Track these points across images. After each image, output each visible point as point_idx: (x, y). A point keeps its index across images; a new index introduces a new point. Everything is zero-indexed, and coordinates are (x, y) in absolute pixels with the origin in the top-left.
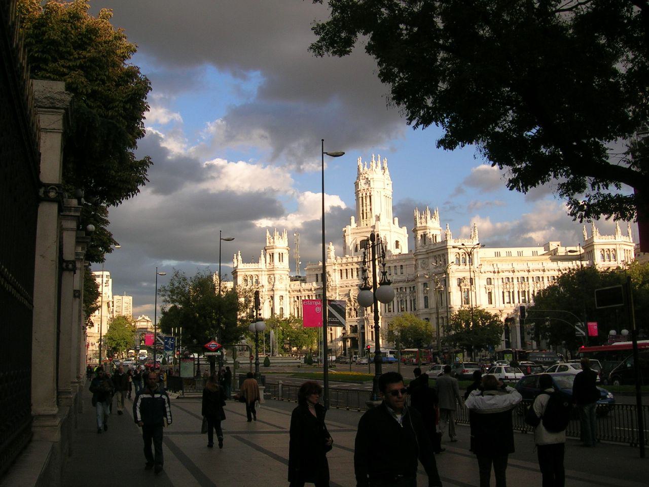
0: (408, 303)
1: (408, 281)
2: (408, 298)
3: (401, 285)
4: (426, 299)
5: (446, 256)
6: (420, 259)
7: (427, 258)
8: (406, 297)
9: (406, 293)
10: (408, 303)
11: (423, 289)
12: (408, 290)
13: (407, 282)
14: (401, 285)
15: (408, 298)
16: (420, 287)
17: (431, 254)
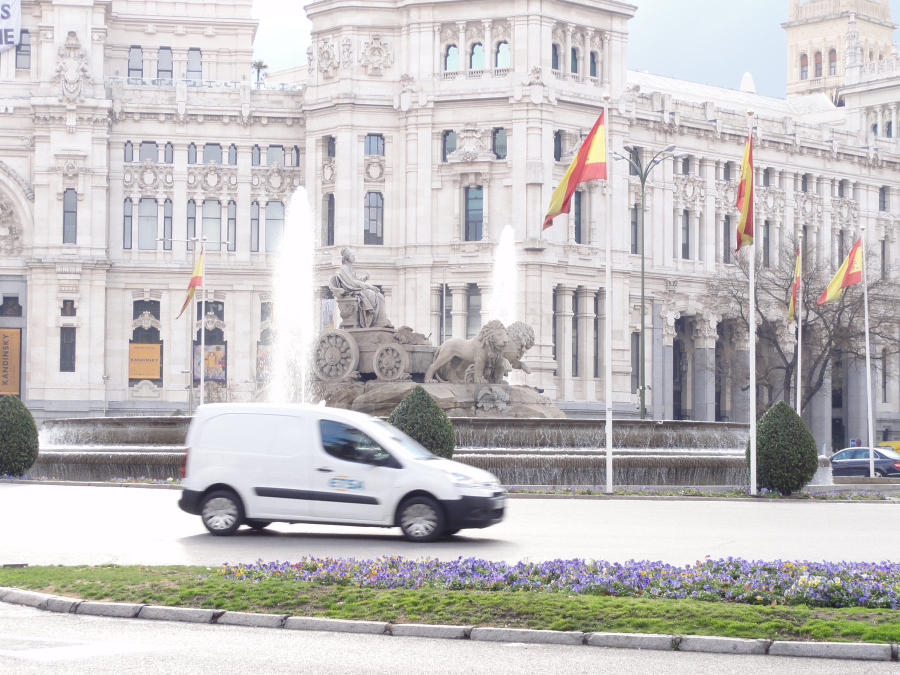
0: (244, 213)
1: (254, 120)
2: (244, 195)
3: (212, 132)
4: (375, 203)
5: (519, 31)
6: (360, 28)
7: (391, 28)
8: (233, 188)
9: (233, 173)
10: (244, 213)
11: (362, 162)
12: (245, 160)
13: (246, 125)
14: (212, 132)
15: (244, 195)
16: (351, 150)
17: (427, 15)
